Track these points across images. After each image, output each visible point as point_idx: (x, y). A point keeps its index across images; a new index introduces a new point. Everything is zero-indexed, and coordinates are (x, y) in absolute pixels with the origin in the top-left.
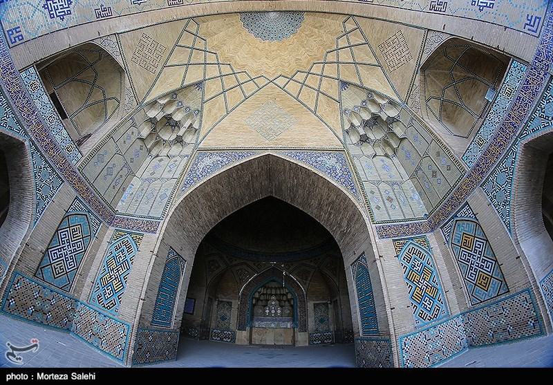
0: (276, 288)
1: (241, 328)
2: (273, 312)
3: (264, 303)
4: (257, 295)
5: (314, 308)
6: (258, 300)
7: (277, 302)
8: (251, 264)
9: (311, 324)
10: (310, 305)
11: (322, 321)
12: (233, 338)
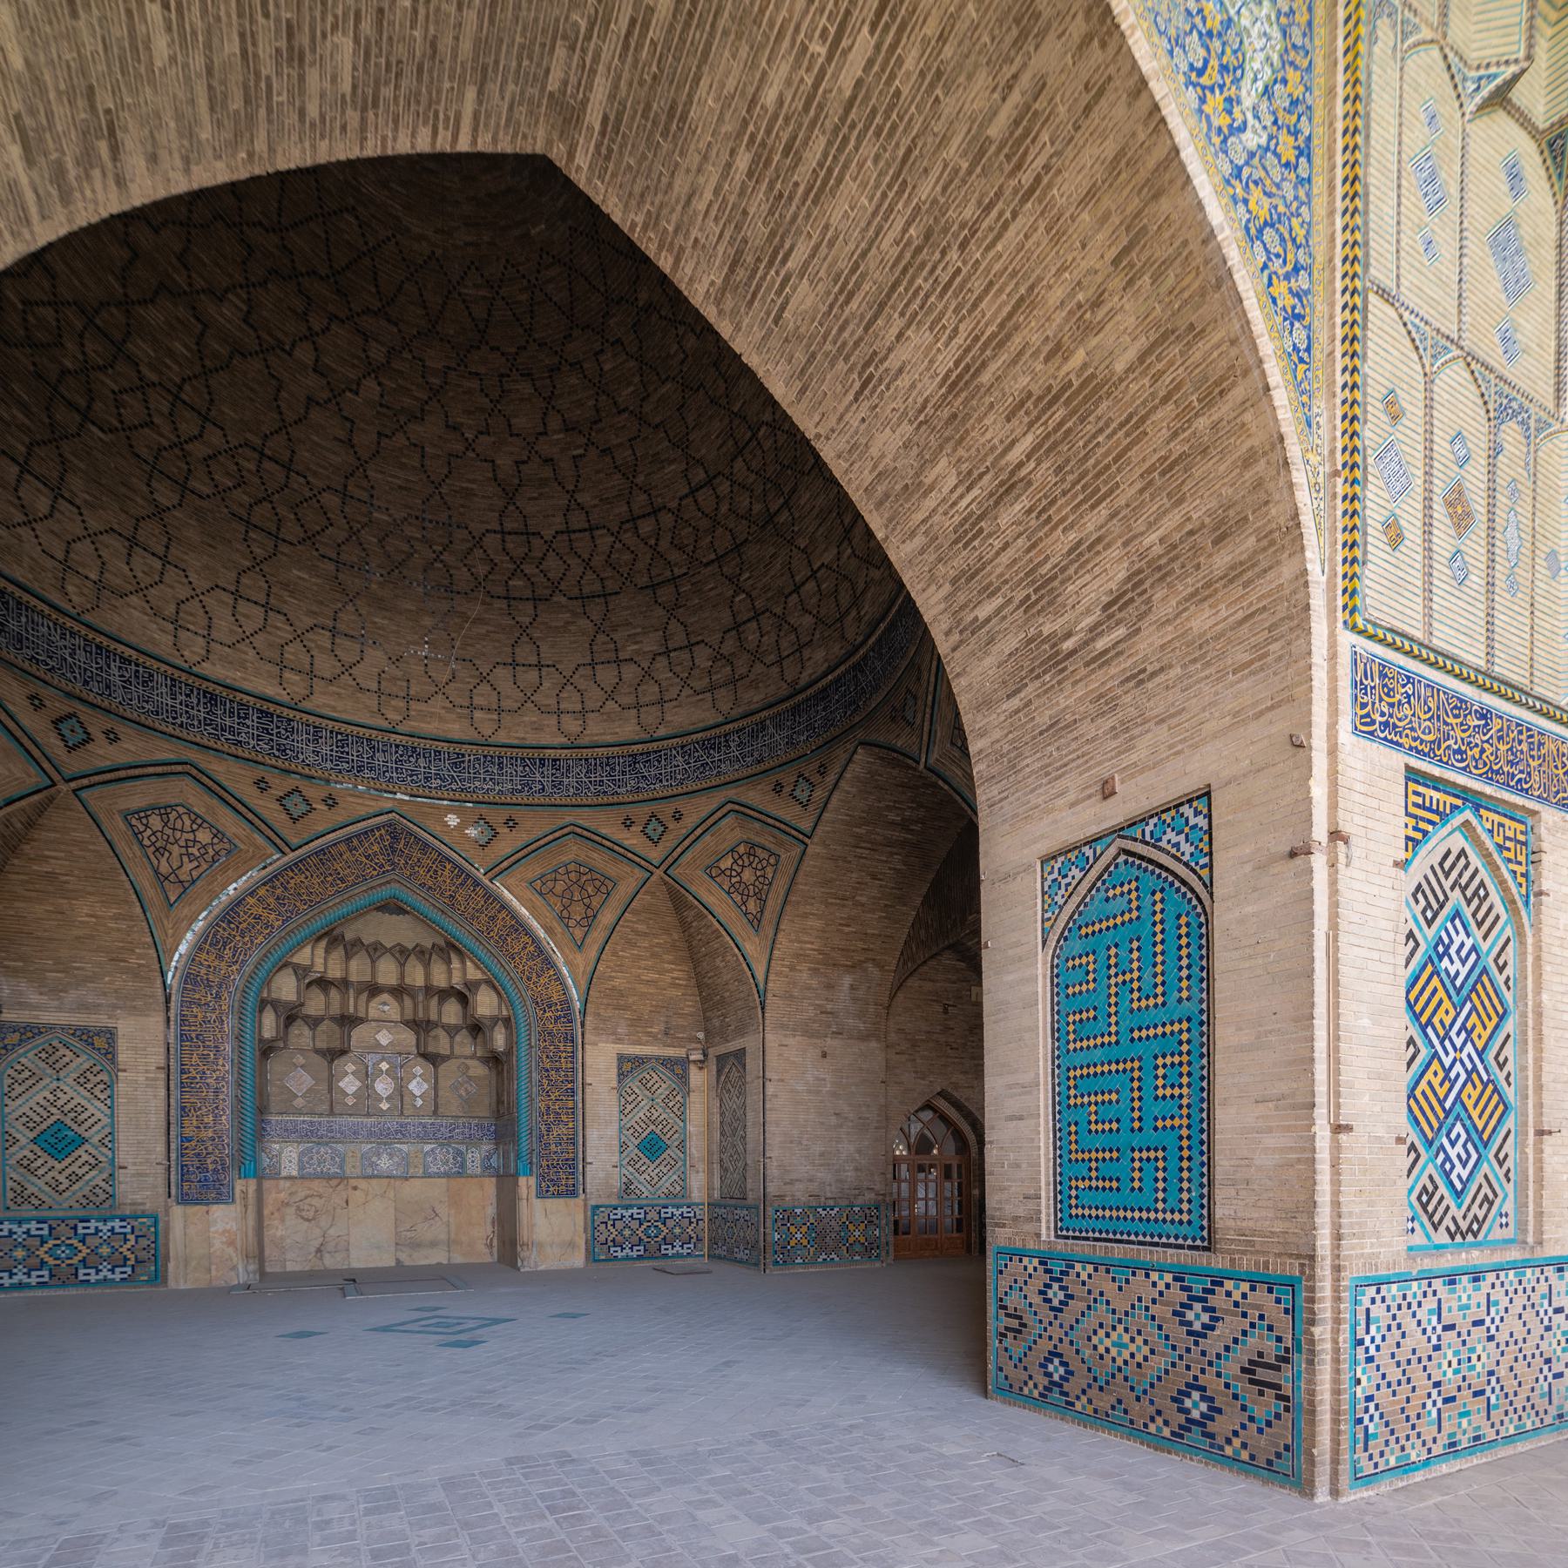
0: (402, 954)
1: (197, 1179)
2: (383, 1087)
3: (327, 1035)
4: (286, 987)
5: (621, 1075)
6: (291, 1016)
7: (408, 1037)
8: (238, 778)
9: (603, 1154)
10: (600, 1060)
11: (652, 1147)
12: (145, 1259)
